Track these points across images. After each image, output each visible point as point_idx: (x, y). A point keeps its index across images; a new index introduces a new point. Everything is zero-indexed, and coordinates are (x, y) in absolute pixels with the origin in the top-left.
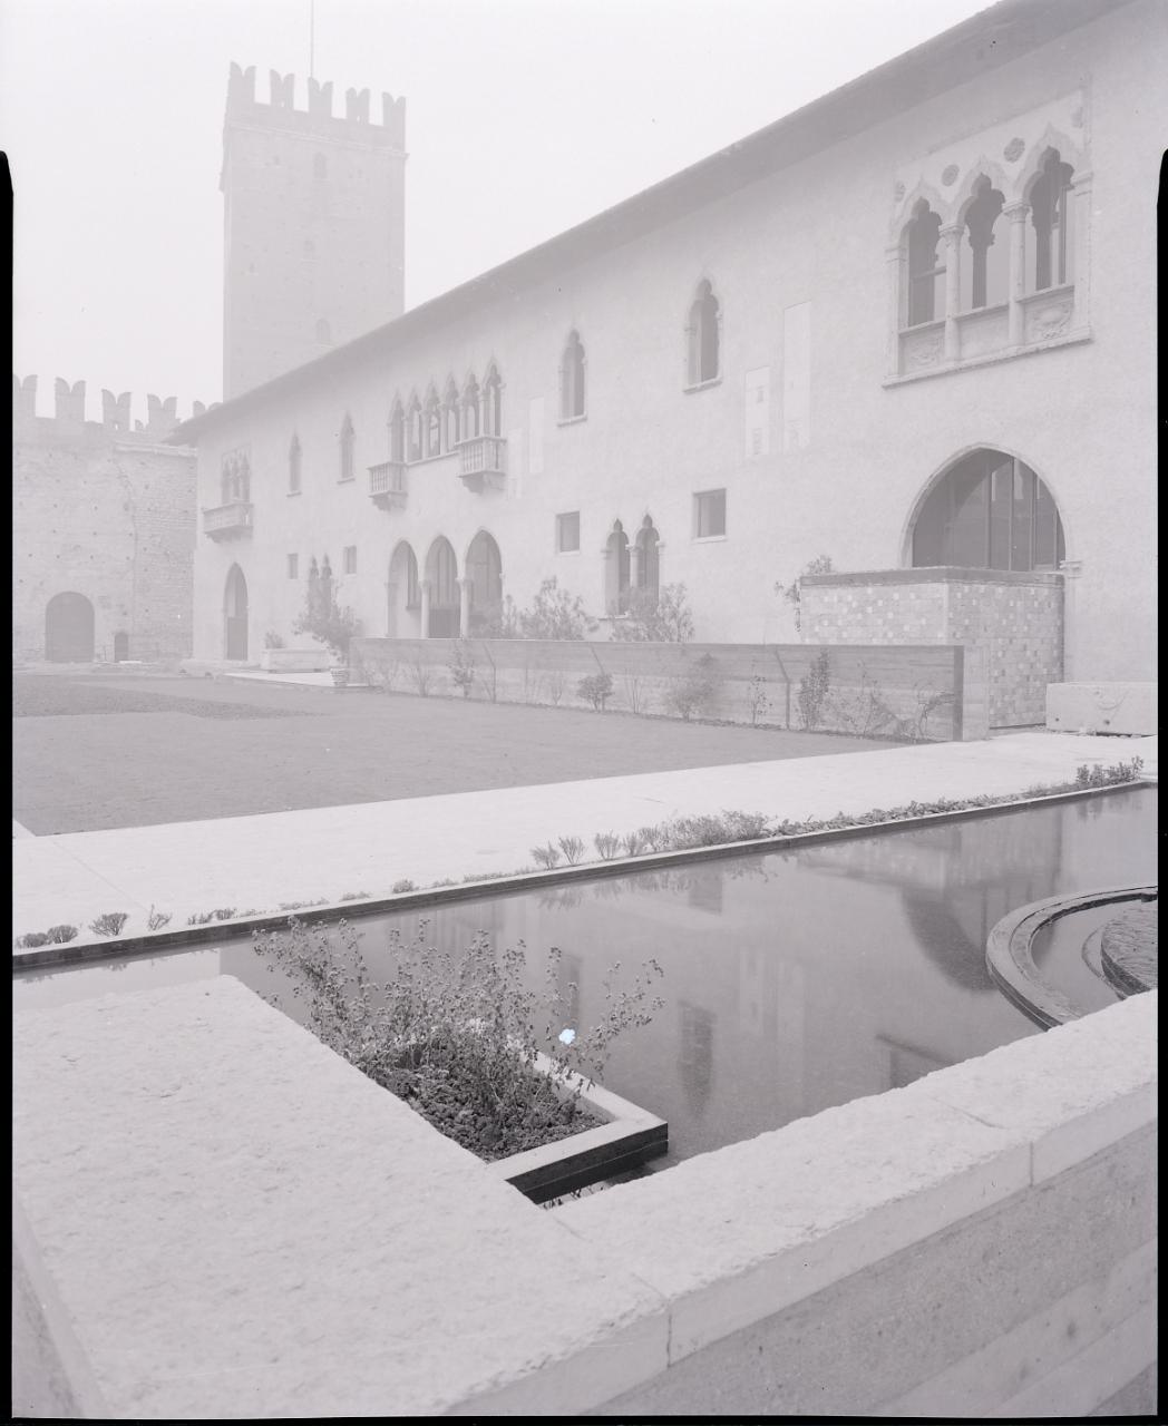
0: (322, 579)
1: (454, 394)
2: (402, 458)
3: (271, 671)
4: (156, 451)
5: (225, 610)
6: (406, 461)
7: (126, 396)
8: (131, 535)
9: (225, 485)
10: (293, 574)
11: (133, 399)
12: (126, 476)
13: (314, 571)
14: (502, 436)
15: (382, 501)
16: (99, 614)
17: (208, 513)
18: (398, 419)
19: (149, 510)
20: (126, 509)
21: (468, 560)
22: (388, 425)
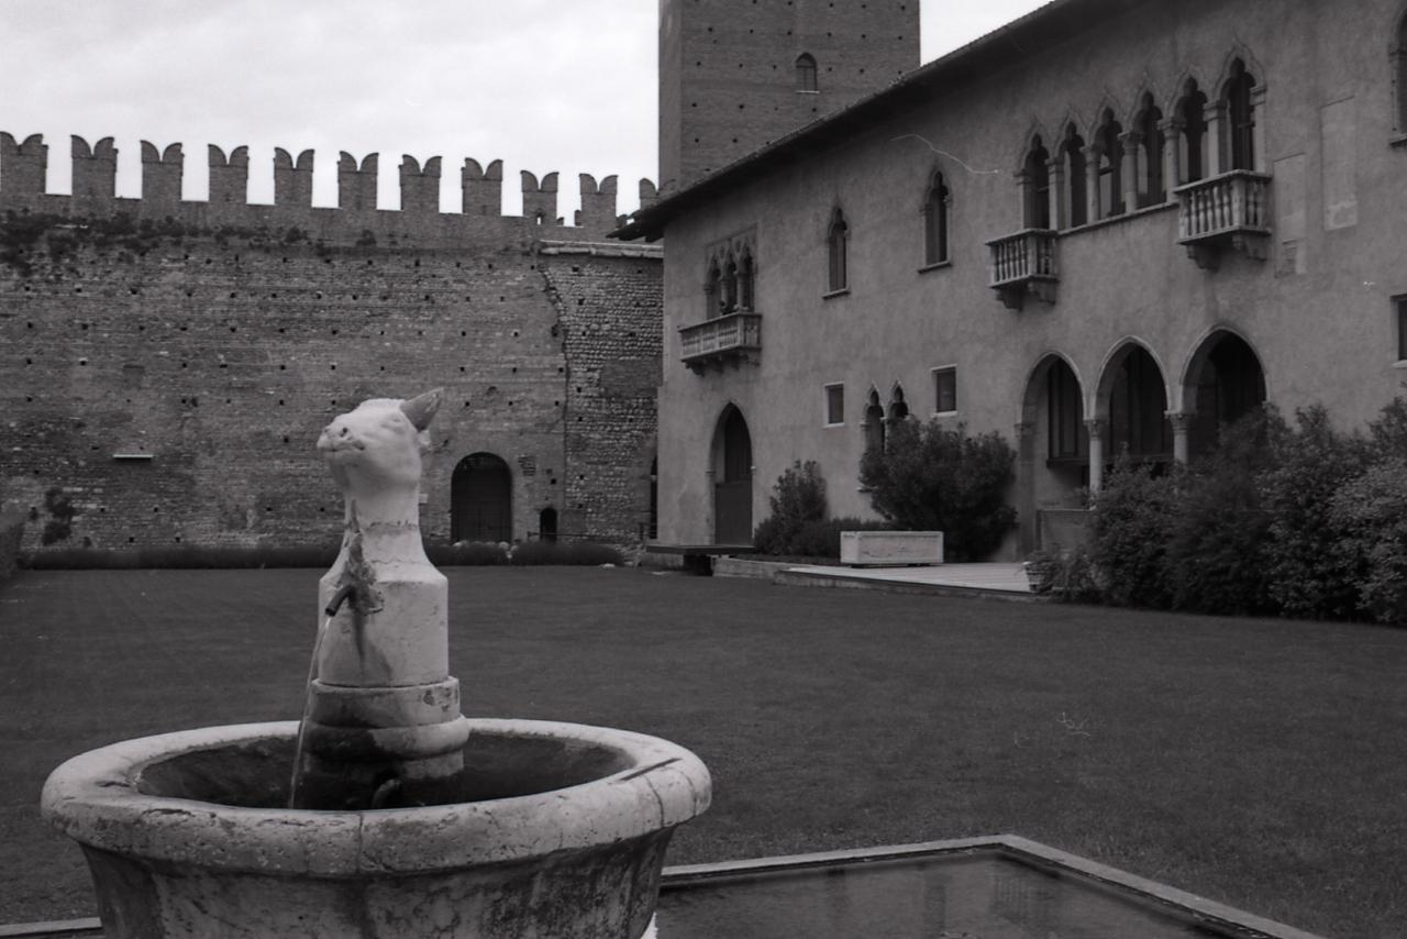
0: (889, 422)
1: (1150, 113)
2: (1046, 224)
3: (855, 566)
4: (594, 251)
5: (712, 474)
6: (1053, 226)
7: (552, 178)
8: (561, 370)
9: (711, 290)
10: (836, 413)
11: (561, 180)
12: (554, 289)
13: (874, 410)
14: (1261, 168)
15: (1014, 296)
16: (520, 483)
17: (688, 333)
18: (1036, 168)
19: (584, 334)
20: (555, 335)
21: (1188, 381)
22: (1017, 176)
